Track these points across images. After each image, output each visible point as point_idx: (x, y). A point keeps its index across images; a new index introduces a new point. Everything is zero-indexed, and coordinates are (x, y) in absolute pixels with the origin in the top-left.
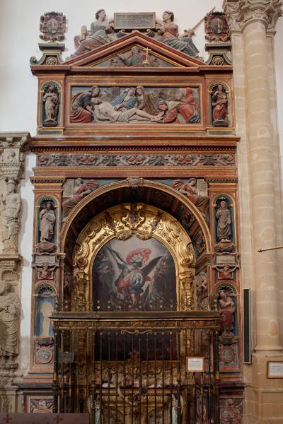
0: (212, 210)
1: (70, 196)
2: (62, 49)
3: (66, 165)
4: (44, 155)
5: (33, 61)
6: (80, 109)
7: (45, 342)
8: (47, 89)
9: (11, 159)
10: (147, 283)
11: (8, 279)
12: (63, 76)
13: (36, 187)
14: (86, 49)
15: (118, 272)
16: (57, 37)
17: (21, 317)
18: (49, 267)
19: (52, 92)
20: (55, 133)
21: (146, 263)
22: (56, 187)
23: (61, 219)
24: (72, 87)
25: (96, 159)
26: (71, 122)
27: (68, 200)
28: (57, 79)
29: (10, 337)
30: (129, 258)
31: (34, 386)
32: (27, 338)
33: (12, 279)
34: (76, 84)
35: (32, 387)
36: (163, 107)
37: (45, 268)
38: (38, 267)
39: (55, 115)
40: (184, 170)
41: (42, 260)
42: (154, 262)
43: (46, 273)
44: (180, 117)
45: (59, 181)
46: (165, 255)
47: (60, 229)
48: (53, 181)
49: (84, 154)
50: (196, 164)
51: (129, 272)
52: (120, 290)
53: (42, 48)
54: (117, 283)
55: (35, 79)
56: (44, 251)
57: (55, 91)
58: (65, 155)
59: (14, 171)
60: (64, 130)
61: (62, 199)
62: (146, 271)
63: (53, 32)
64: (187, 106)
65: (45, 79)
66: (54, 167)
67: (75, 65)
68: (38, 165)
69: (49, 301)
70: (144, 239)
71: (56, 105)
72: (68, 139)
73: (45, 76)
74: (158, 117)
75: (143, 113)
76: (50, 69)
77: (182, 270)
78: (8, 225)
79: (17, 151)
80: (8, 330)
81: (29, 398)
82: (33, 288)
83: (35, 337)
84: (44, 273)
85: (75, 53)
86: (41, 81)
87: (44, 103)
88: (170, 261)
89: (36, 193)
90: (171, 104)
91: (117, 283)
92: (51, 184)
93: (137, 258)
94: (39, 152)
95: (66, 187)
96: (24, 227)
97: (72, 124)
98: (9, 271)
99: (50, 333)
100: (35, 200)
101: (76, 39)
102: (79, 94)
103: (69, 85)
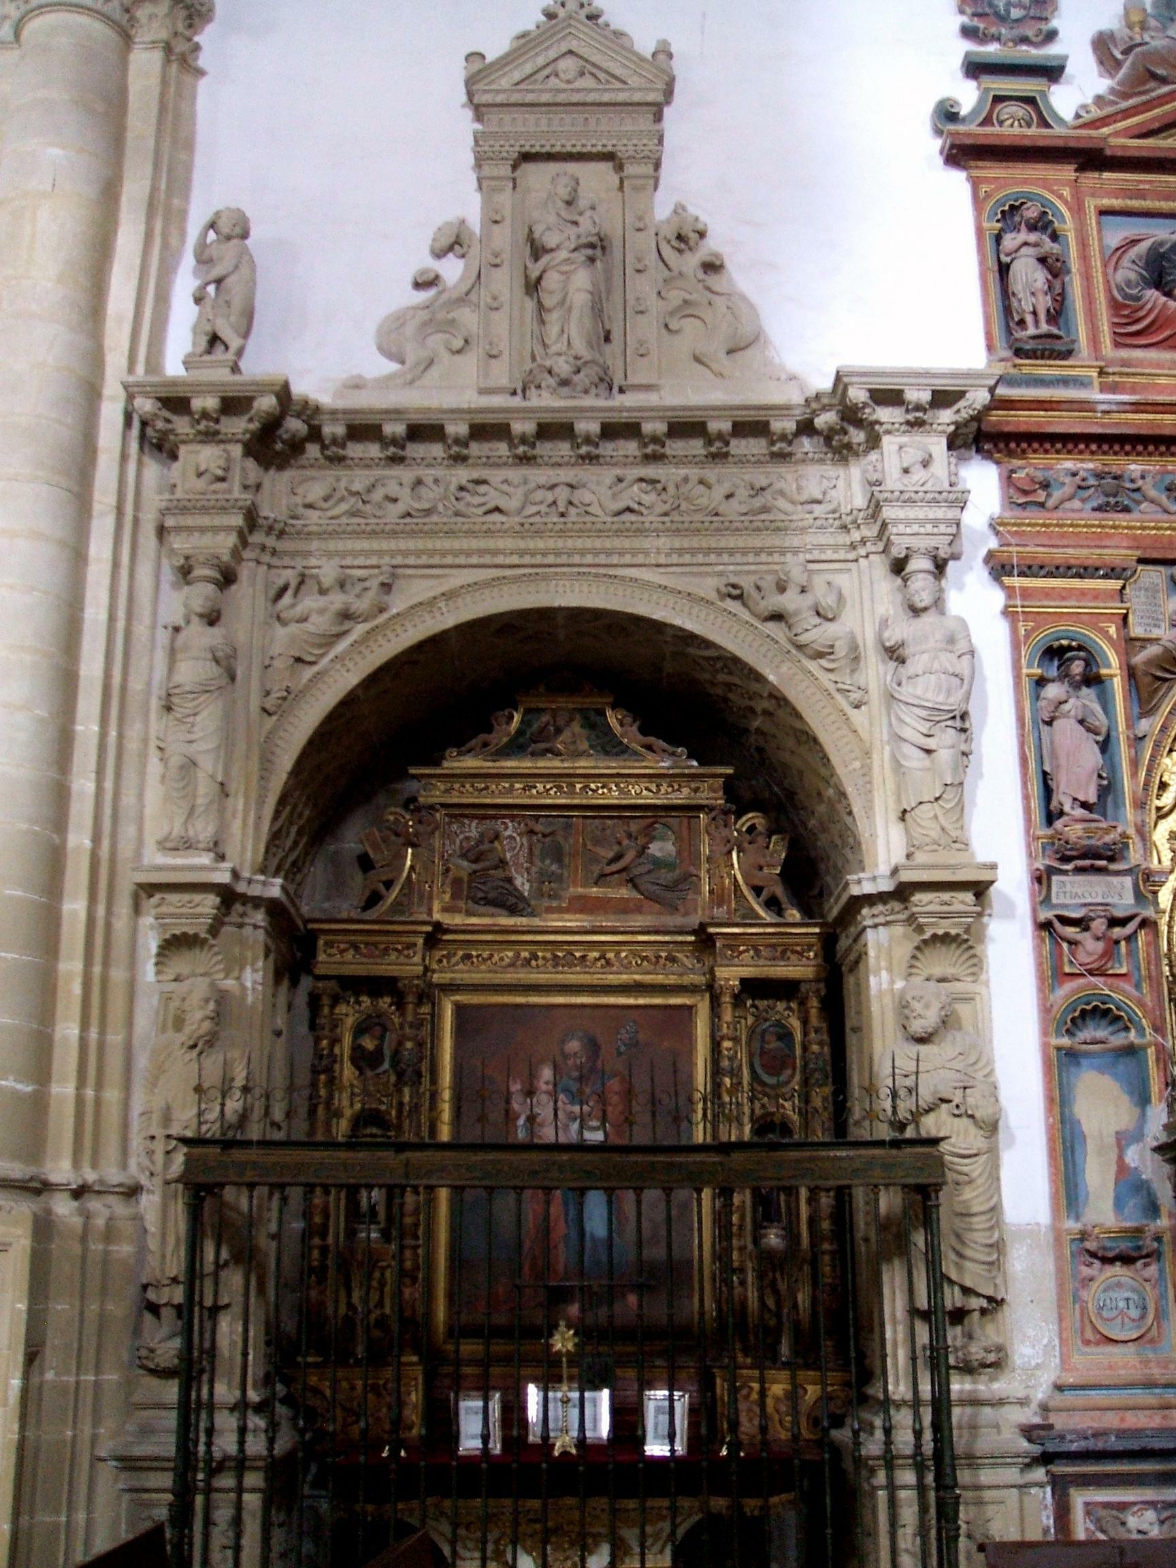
1: (1156, 633)
2: (1052, 72)
3: (1126, 509)
4: (1033, 465)
5: (947, 114)
6: (1152, 295)
7: (1124, 1246)
8: (1010, 214)
9: (919, 475)
11: (938, 971)
12: (1067, 172)
14: (1154, 76)
16: (1030, 33)
17: (1002, 1135)
18: (1114, 922)
19: (1032, 227)
20: (1065, 382)
22: (1097, 595)
23: (1130, 725)
24: (1103, 212)
26: (1117, 345)
27: (1153, 650)
28: (1046, 184)
29: (979, 1222)
31: (1113, 1443)
32: (1029, 1232)
33: (950, 971)
34: (1117, 203)
35: (1100, 1445)
37: (1099, 925)
39: (1057, 313)
43: (1100, 946)
45: (1112, 572)
47: (1135, 763)
48: (1085, 571)
53: (975, 69)
55: (958, 181)
56: (1083, 856)
57: (1041, 224)
58: (1115, 469)
59: (936, 522)
60: (1102, 373)
61: (1130, 644)
63: (1016, 13)
65: (1006, 182)
66: (1080, 512)
67: (1117, 134)
68: (1009, 503)
69: (1101, 1070)
71: (1055, 276)
72: (1138, 407)
73: (993, 171)
76: (1027, 143)
78: (931, 743)
79: (938, 446)
80: (968, 1194)
81: (1079, 1499)
82: (1045, 1009)
83: (1071, 1225)
84: (1091, 947)
85: (1112, 91)
86: (984, 188)
87: (1004, 270)
92: (1076, 583)
94: (1011, 454)
95: (1136, 599)
96: (980, 758)
97: (1124, 353)
98: (945, 939)
99: (1119, 1204)
100: (1016, 646)
101: (1102, 45)
102: (1134, 242)
103: (1091, 205)
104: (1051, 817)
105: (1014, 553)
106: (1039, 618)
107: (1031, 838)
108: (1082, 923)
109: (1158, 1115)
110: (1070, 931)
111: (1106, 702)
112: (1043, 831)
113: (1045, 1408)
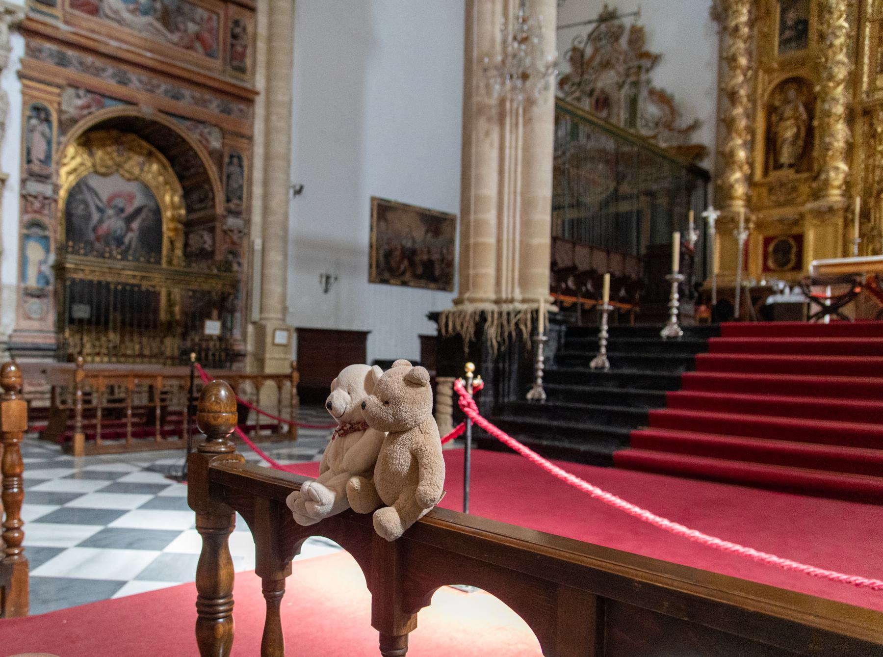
0: (225, 165)
7: (38, 293)
10: (130, 235)
13: (25, 86)
15: (96, 216)
18: (46, 198)
21: (130, 210)
25: (103, 70)
30: (110, 200)
36: (182, 27)
37: (40, 198)
38: (30, 195)
40: (199, 112)
41: (34, 187)
42: (138, 211)
44: (198, 45)
45: (59, 86)
46: (152, 204)
47: (57, 150)
48: (49, 84)
49: (89, 59)
50: (214, 106)
51: (109, 217)
52: (98, 239)
54: (95, 229)
61: (60, 112)
62: (129, 220)
64: (207, 36)
66: (50, 65)
68: (27, 54)
70: (129, 180)
72: (75, 34)
74: (175, 37)
75: (158, 25)
77: (172, 225)
84: (37, 205)
88: (157, 212)
89: (24, 94)
90: (192, 27)
91: (95, 229)
93: (119, 202)
99: (38, 281)
100: (24, 103)
104: (29, 161)
105: (28, 72)
106: (32, 97)
107: (22, 167)
108: (35, 197)
109: (52, 258)
110: (31, 199)
111: (50, 127)
112: (26, 166)
113: (10, 336)
